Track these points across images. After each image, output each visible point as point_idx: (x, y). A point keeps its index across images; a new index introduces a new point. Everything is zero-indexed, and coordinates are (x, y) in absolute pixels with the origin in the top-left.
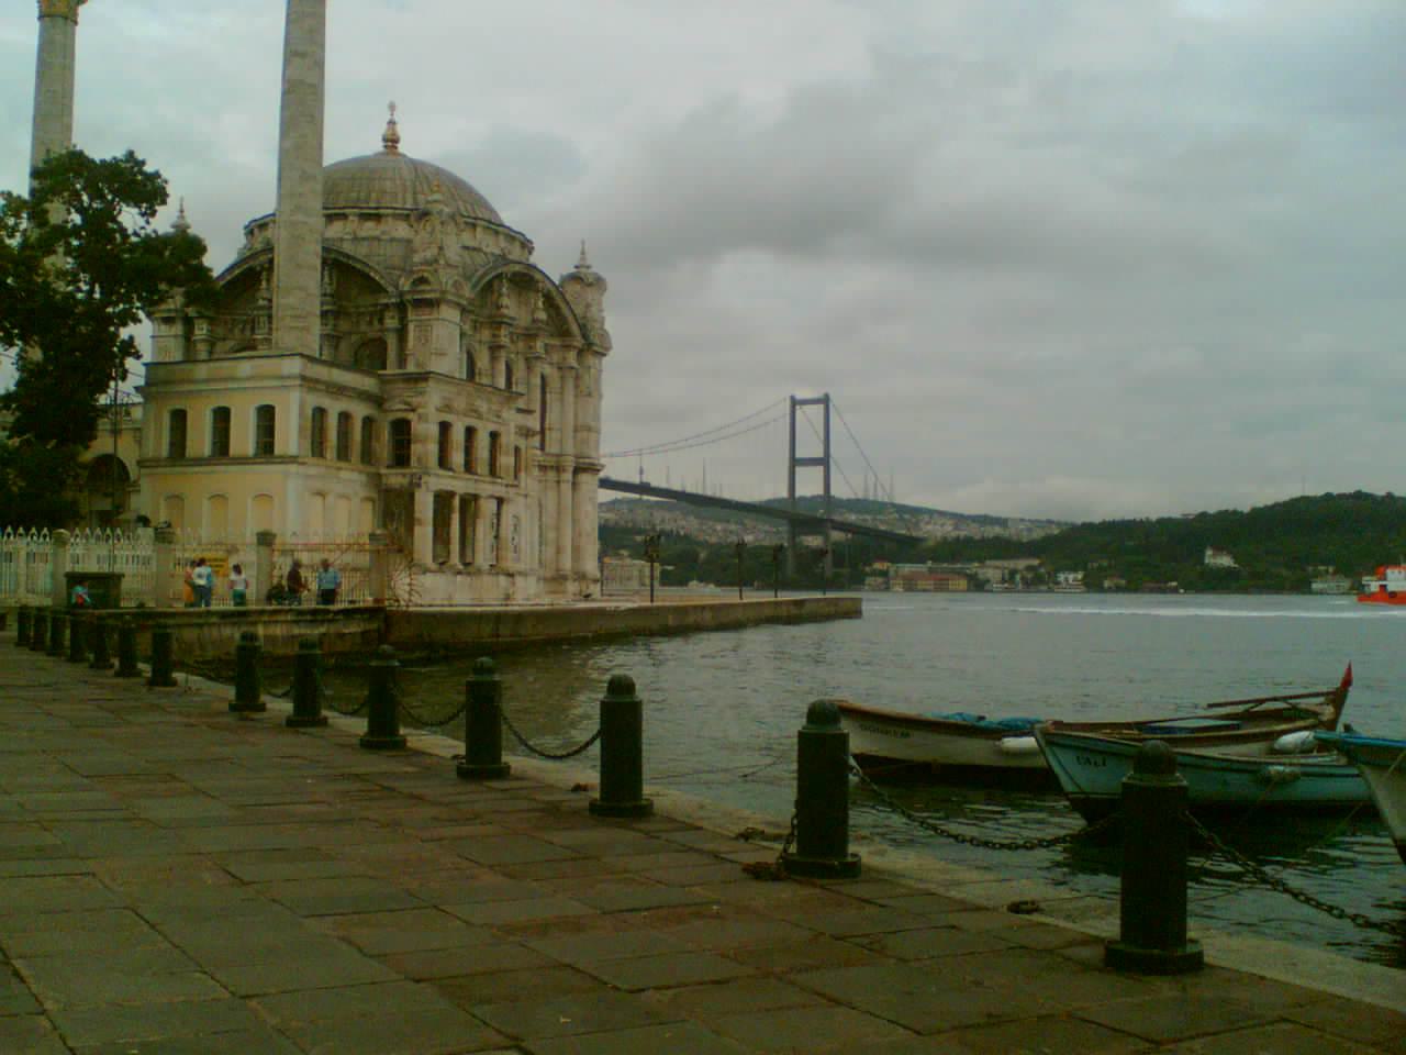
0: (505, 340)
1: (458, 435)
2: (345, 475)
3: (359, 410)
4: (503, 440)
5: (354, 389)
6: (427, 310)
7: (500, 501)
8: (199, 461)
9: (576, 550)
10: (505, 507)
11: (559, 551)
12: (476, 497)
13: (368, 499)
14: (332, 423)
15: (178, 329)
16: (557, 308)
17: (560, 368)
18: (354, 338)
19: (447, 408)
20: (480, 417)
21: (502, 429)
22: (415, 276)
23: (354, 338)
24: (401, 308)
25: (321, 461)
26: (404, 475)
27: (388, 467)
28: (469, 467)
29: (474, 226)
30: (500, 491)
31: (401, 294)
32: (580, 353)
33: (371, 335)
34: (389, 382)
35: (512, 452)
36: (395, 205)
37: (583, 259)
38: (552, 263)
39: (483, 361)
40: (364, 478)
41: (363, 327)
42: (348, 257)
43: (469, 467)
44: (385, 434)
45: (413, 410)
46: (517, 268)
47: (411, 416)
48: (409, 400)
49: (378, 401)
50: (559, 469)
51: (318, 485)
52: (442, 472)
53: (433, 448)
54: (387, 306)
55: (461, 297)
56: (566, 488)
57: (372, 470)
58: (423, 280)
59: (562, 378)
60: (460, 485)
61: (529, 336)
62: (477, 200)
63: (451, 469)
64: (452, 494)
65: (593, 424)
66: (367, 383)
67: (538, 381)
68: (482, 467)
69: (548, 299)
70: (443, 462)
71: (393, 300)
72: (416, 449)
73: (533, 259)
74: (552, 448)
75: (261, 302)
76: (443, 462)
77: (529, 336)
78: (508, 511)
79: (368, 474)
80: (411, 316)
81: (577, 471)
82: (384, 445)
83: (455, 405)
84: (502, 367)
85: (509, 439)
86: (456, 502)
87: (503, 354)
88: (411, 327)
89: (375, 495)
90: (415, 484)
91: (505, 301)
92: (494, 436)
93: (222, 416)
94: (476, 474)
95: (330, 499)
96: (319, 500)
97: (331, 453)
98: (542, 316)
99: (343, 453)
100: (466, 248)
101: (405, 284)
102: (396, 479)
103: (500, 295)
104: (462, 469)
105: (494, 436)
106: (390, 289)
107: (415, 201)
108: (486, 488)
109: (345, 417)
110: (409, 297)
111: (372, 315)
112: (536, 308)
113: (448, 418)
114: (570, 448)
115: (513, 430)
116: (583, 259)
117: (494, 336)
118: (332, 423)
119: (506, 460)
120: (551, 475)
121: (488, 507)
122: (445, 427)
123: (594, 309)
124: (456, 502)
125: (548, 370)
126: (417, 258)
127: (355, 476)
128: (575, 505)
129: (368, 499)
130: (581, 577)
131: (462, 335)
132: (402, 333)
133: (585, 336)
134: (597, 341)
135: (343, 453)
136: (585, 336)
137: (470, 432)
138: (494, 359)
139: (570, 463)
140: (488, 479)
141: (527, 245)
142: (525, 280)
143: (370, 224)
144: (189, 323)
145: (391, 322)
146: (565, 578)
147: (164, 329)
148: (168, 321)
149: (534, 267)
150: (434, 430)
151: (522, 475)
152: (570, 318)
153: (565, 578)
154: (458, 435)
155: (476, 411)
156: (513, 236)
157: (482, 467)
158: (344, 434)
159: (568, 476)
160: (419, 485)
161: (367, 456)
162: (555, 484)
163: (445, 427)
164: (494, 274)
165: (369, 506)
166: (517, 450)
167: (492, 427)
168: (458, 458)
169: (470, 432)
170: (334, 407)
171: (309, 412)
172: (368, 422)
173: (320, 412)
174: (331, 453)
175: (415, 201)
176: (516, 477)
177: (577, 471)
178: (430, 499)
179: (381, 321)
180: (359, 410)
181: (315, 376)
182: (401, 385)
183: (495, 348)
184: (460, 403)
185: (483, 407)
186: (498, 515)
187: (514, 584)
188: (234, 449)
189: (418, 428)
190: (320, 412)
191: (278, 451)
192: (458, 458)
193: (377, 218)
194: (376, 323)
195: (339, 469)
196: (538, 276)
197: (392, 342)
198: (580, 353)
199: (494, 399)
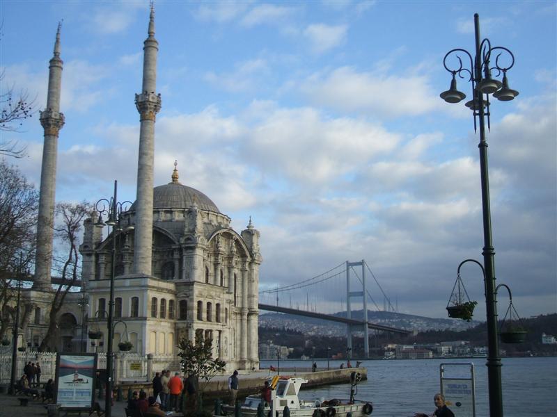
0: (220, 261)
1: (204, 306)
2: (163, 324)
3: (169, 297)
4: (221, 306)
5: (167, 289)
6: (191, 251)
7: (220, 332)
9: (249, 349)
10: (222, 335)
11: (242, 350)
12: (211, 331)
13: (172, 333)
14: (159, 303)
15: (93, 258)
16: (240, 245)
17: (241, 270)
18: (161, 262)
19: (201, 295)
20: (212, 298)
21: (221, 303)
22: (186, 237)
23: (161, 262)
24: (180, 250)
25: (154, 319)
26: (184, 323)
27: (179, 320)
28: (209, 319)
29: (208, 214)
30: (220, 328)
31: (180, 245)
32: (250, 264)
34: (180, 286)
36: (177, 206)
37: (250, 224)
38: (238, 227)
39: (211, 271)
40: (169, 325)
41: (165, 257)
42: (159, 228)
43: (209, 319)
44: (177, 307)
45: (188, 297)
46: (225, 230)
47: (187, 299)
48: (188, 293)
49: (175, 294)
50: (241, 314)
51: (153, 328)
52: (200, 322)
53: (195, 312)
54: (175, 249)
55: (203, 245)
56: (245, 322)
57: (172, 321)
58: (189, 239)
59: (243, 275)
60: (204, 326)
61: (230, 258)
62: (211, 203)
63: (202, 320)
64: (203, 330)
65: (255, 294)
66: (171, 286)
67: (233, 277)
68: (213, 319)
69: (237, 241)
70: (199, 318)
71: (177, 247)
72: (189, 312)
73: (231, 225)
74: (239, 305)
75: (126, 247)
76: (199, 318)
77: (230, 258)
78: (223, 335)
79: (171, 323)
80: (184, 254)
81: (249, 315)
82: (177, 312)
83: (203, 294)
84: (219, 273)
85: (224, 305)
86: (204, 333)
87: (219, 267)
88: (184, 258)
89: (173, 331)
90: (189, 327)
91: (220, 244)
92: (218, 305)
94: (211, 321)
95: (158, 333)
96: (154, 334)
97: (158, 315)
98: (235, 250)
99: (163, 316)
100: (205, 223)
101: (182, 240)
102: (182, 325)
103: (218, 242)
104: (206, 320)
105: (218, 305)
106: (177, 243)
107: (186, 205)
108: (215, 327)
109: (163, 301)
110: (183, 246)
111: (169, 252)
112: (232, 246)
113: (200, 299)
114: (246, 305)
115: (225, 301)
116: (250, 224)
117: (216, 259)
118: (159, 303)
119: (222, 315)
120: (239, 317)
121: (216, 334)
122: (200, 303)
123: (255, 245)
124: (204, 333)
126: (186, 230)
127: (166, 324)
128: (249, 329)
129: (172, 333)
130: (251, 361)
131: (204, 260)
132: (181, 261)
133: (252, 256)
134: (256, 258)
135: (163, 316)
136: (252, 256)
137: (209, 304)
138: (216, 269)
139: (246, 312)
140: (216, 323)
141: (229, 220)
142: (228, 235)
143: (169, 215)
144: (97, 256)
145: (176, 256)
146: (245, 362)
147: (87, 258)
148: (89, 255)
149: (231, 229)
150: (195, 304)
151: (228, 320)
152: (246, 250)
153: (245, 362)
154: (204, 306)
155: (211, 296)
156: (224, 217)
157: (213, 319)
158: (163, 308)
159: (245, 317)
160: (190, 327)
161: (171, 316)
162: (239, 321)
163: (200, 303)
164: (216, 234)
165: (171, 335)
166: (226, 309)
167: (217, 302)
168: (204, 315)
169: (209, 304)
170: (159, 296)
171: (151, 300)
172: (171, 301)
173: (155, 299)
174: (158, 315)
175: (186, 205)
176: (226, 322)
177: (249, 315)
178: (194, 332)
179: (172, 254)
180: (169, 297)
181: (153, 285)
182: (183, 287)
183: (216, 264)
184: (205, 293)
185: (213, 294)
186: (219, 337)
188: (123, 315)
189: (189, 304)
190: (155, 299)
191: (139, 315)
192: (204, 315)
193: (171, 212)
194: (170, 256)
195: (161, 321)
196: (233, 233)
197: (177, 263)
198: (250, 264)
199: (218, 290)
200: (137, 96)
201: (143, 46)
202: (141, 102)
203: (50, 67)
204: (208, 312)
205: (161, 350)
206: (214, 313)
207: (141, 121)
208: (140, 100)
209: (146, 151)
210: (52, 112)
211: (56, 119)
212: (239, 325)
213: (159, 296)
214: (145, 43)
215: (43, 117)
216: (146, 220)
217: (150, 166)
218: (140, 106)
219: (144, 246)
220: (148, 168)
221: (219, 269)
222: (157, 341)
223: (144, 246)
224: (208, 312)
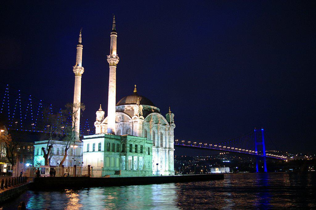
1: (134, 146)
6: (136, 123)
33: (129, 127)
35: (147, 149)
53: (128, 149)
74: (164, 146)
93: (94, 145)
99: (113, 151)
122: (131, 145)
125: (163, 132)
137: (136, 146)
139: (167, 150)
150: (128, 145)
159: (167, 152)
162: (164, 153)
168: (134, 150)
169: (136, 146)
171: (106, 144)
172: (118, 145)
187: (146, 173)
192: (134, 150)
197: (131, 128)
204: (136, 149)
205: (112, 165)
206: (139, 149)
212: (164, 155)
221: (152, 130)
222: (110, 162)
224: (136, 149)
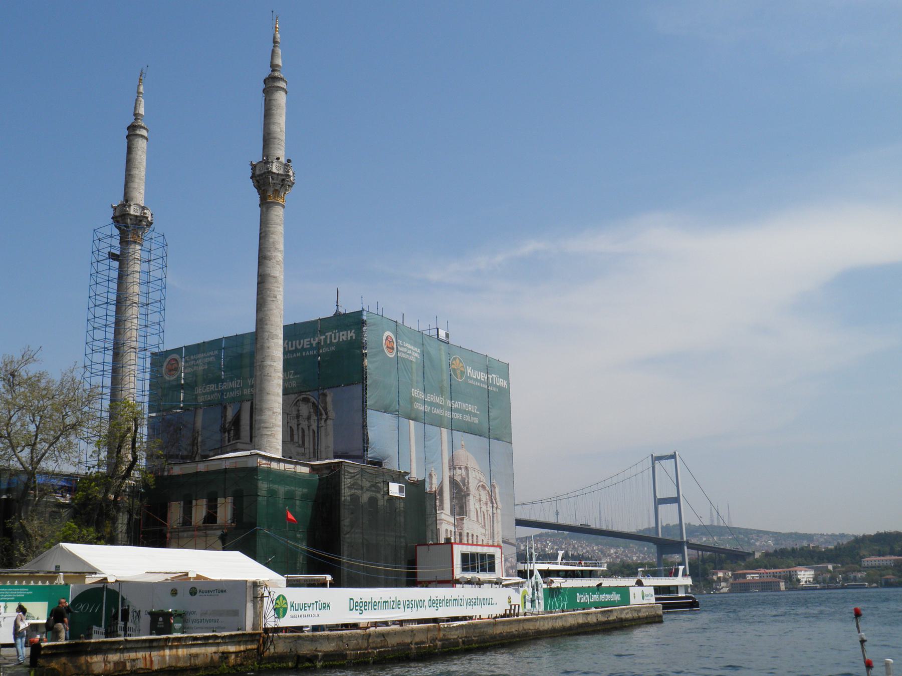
8: (198, 529)
200: (254, 167)
201: (263, 86)
202: (259, 176)
203: (128, 137)
207: (260, 206)
208: (258, 172)
209: (269, 254)
210: (130, 206)
211: (136, 216)
213: (282, 490)
214: (265, 81)
215: (117, 214)
216: (271, 366)
217: (274, 277)
218: (258, 181)
219: (266, 409)
220: (271, 280)
223: (266, 409)
